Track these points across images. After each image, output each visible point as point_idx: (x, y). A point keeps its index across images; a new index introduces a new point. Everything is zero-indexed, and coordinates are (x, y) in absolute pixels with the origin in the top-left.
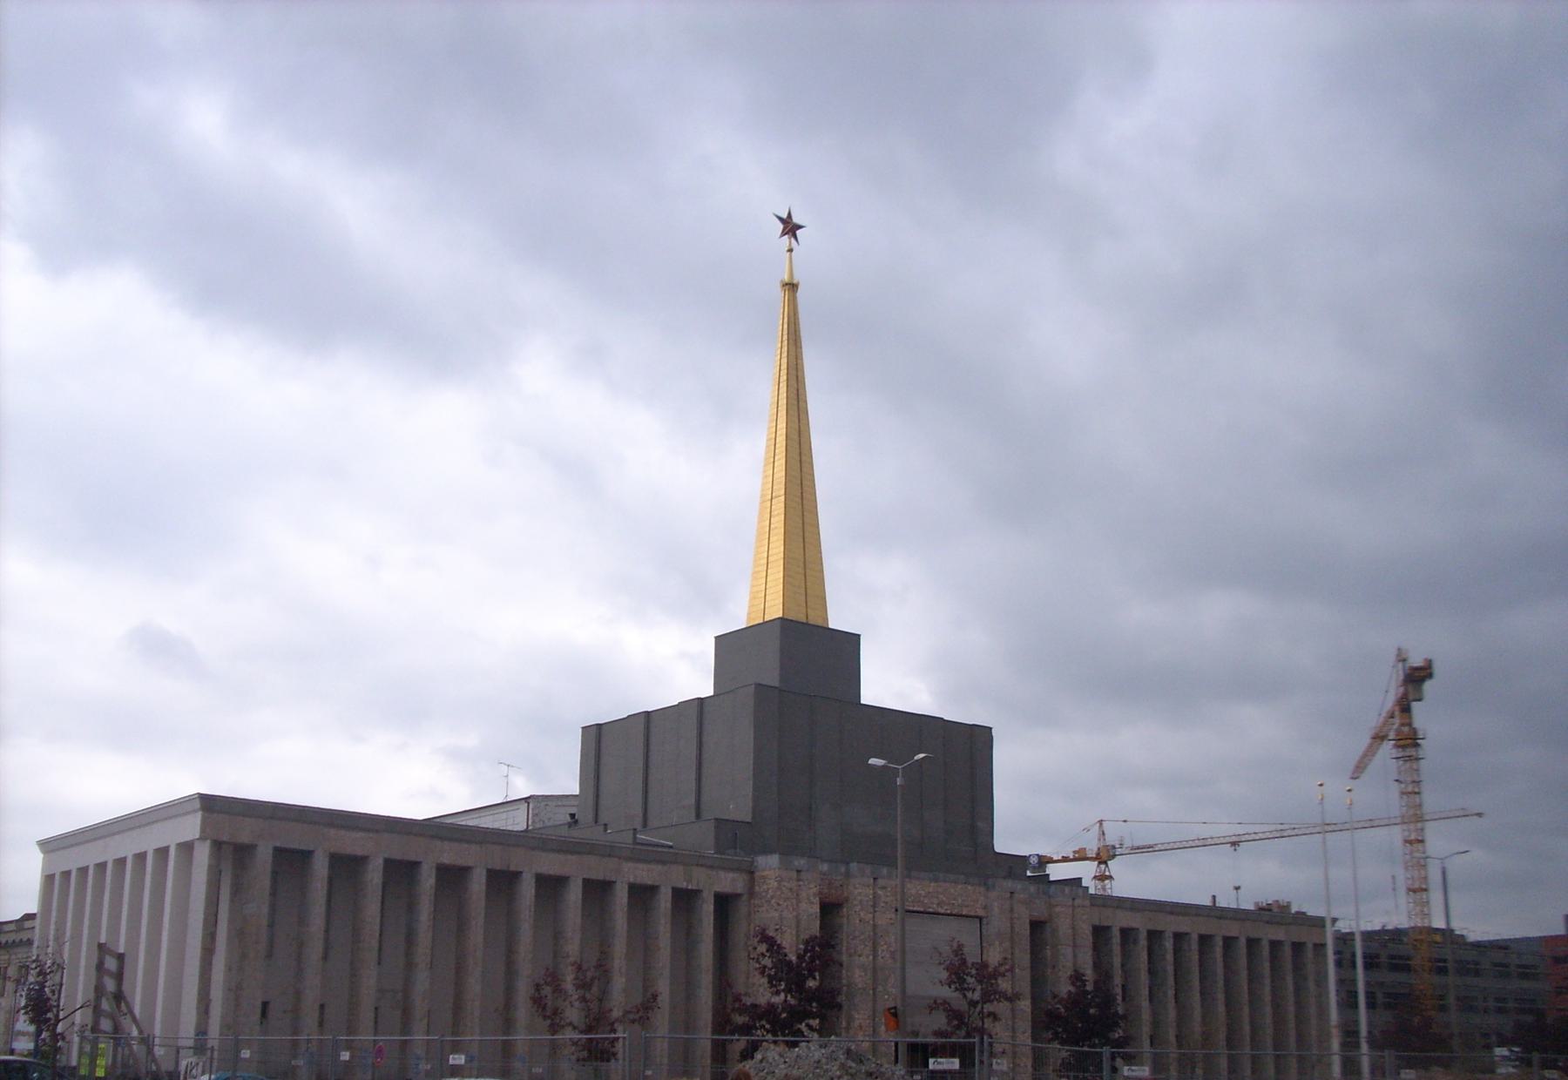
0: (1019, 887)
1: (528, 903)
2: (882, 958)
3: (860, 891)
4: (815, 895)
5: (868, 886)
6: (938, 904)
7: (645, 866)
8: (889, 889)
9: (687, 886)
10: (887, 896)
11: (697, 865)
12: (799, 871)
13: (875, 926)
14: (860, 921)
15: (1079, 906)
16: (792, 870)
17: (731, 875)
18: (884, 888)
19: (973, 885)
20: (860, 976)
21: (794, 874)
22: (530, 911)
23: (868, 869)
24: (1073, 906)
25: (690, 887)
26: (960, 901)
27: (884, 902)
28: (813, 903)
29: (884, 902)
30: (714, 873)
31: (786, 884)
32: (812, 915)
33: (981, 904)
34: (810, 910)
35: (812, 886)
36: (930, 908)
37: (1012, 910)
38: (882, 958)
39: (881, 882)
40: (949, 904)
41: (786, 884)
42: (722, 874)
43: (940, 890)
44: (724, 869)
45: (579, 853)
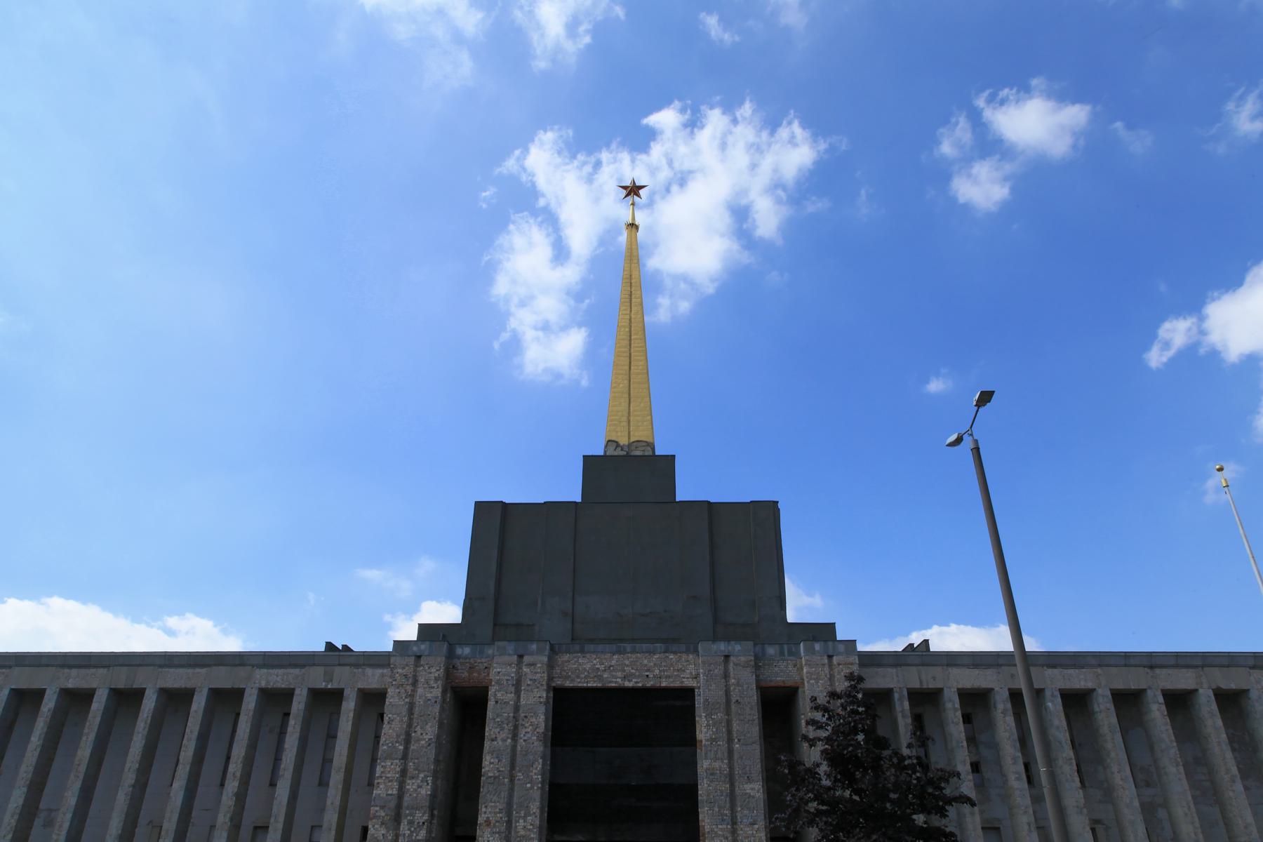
0: (738, 647)
1: (145, 715)
2: (524, 741)
3: (498, 670)
4: (436, 679)
5: (510, 665)
6: (624, 678)
7: (281, 671)
8: (539, 665)
9: (326, 685)
10: (536, 673)
11: (340, 665)
12: (419, 657)
13: (517, 708)
14: (497, 702)
15: (839, 664)
16: (409, 656)
17: (379, 671)
18: (529, 665)
19: (675, 653)
20: (491, 763)
21: (412, 660)
22: (146, 723)
23: (510, 647)
24: (831, 665)
25: (329, 687)
26: (657, 672)
27: (531, 680)
28: (434, 687)
29: (531, 680)
30: (360, 670)
31: (400, 671)
32: (429, 700)
33: (691, 673)
34: (429, 696)
35: (433, 670)
36: (610, 682)
37: (726, 676)
38: (524, 741)
39: (527, 659)
40: (639, 677)
41: (400, 671)
42: (369, 671)
43: (627, 662)
44: (370, 666)
45: (209, 666)
